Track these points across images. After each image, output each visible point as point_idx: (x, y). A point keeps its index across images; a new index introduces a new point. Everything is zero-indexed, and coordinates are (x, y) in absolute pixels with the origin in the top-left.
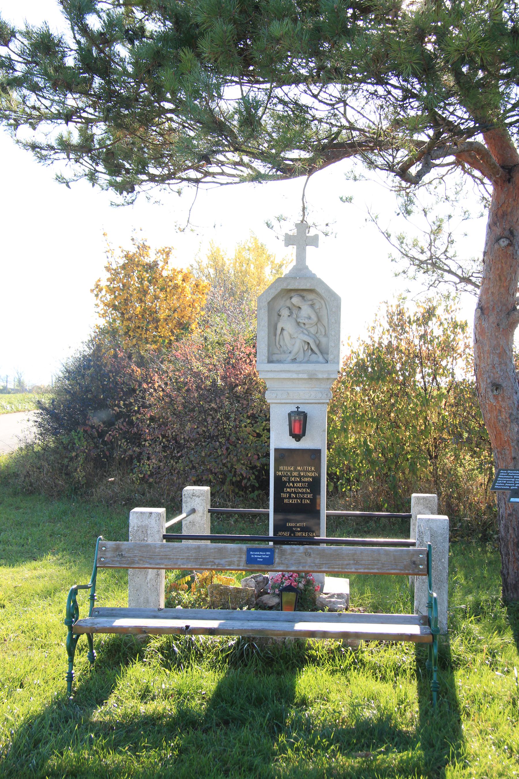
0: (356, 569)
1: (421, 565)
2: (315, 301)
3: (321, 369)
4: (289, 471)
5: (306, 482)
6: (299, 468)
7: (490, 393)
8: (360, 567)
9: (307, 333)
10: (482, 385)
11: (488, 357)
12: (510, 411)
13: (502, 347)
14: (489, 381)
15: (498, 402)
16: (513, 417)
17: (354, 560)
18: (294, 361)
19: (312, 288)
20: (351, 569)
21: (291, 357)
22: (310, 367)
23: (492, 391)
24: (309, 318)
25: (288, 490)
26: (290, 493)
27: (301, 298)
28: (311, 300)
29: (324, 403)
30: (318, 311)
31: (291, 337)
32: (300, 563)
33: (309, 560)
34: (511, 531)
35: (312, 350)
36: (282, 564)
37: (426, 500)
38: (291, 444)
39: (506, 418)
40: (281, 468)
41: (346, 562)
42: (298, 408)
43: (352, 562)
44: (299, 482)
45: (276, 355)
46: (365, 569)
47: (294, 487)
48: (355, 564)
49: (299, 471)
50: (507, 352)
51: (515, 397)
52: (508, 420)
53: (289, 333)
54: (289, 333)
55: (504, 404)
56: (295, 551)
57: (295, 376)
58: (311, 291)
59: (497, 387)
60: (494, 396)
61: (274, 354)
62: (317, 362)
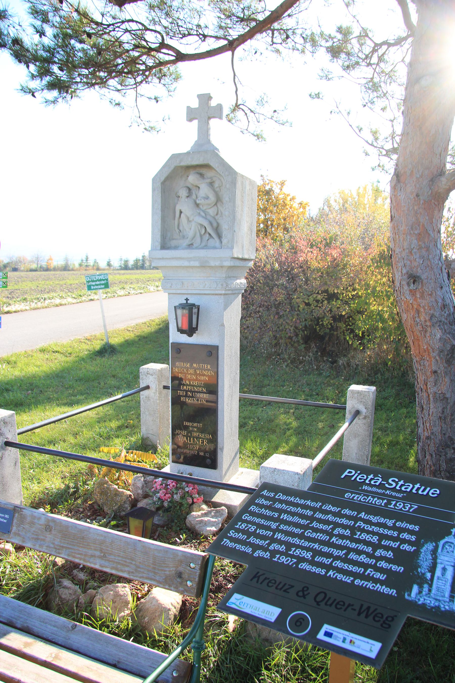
0: (101, 566)
1: (191, 581)
2: (214, 179)
3: (216, 256)
4: (185, 368)
5: (202, 381)
6: (195, 365)
7: (406, 287)
8: (107, 564)
9: (203, 215)
10: (397, 277)
11: (404, 240)
12: (432, 312)
13: (423, 225)
14: (404, 271)
15: (415, 300)
16: (435, 320)
17: (101, 551)
18: (190, 246)
19: (205, 162)
20: (95, 564)
21: (186, 242)
22: (202, 253)
23: (408, 284)
24: (207, 198)
25: (185, 387)
26: (187, 391)
27: (198, 176)
28: (211, 178)
29: (221, 294)
30: (217, 190)
31: (189, 221)
32: (38, 539)
33: (49, 537)
34: (428, 457)
35: (210, 234)
36: (19, 535)
37: (361, 395)
38: (184, 339)
39: (426, 321)
40: (177, 364)
41: (90, 552)
42: (187, 300)
43: (98, 553)
44: (196, 380)
45: (174, 241)
46: (112, 568)
47: (190, 385)
48: (100, 557)
49: (194, 368)
50: (431, 232)
51: (439, 293)
52: (428, 324)
53: (186, 216)
54: (186, 216)
55: (423, 303)
56: (36, 521)
57: (186, 264)
58: (207, 166)
59: (414, 279)
60: (411, 291)
61: (173, 239)
62: (215, 248)
